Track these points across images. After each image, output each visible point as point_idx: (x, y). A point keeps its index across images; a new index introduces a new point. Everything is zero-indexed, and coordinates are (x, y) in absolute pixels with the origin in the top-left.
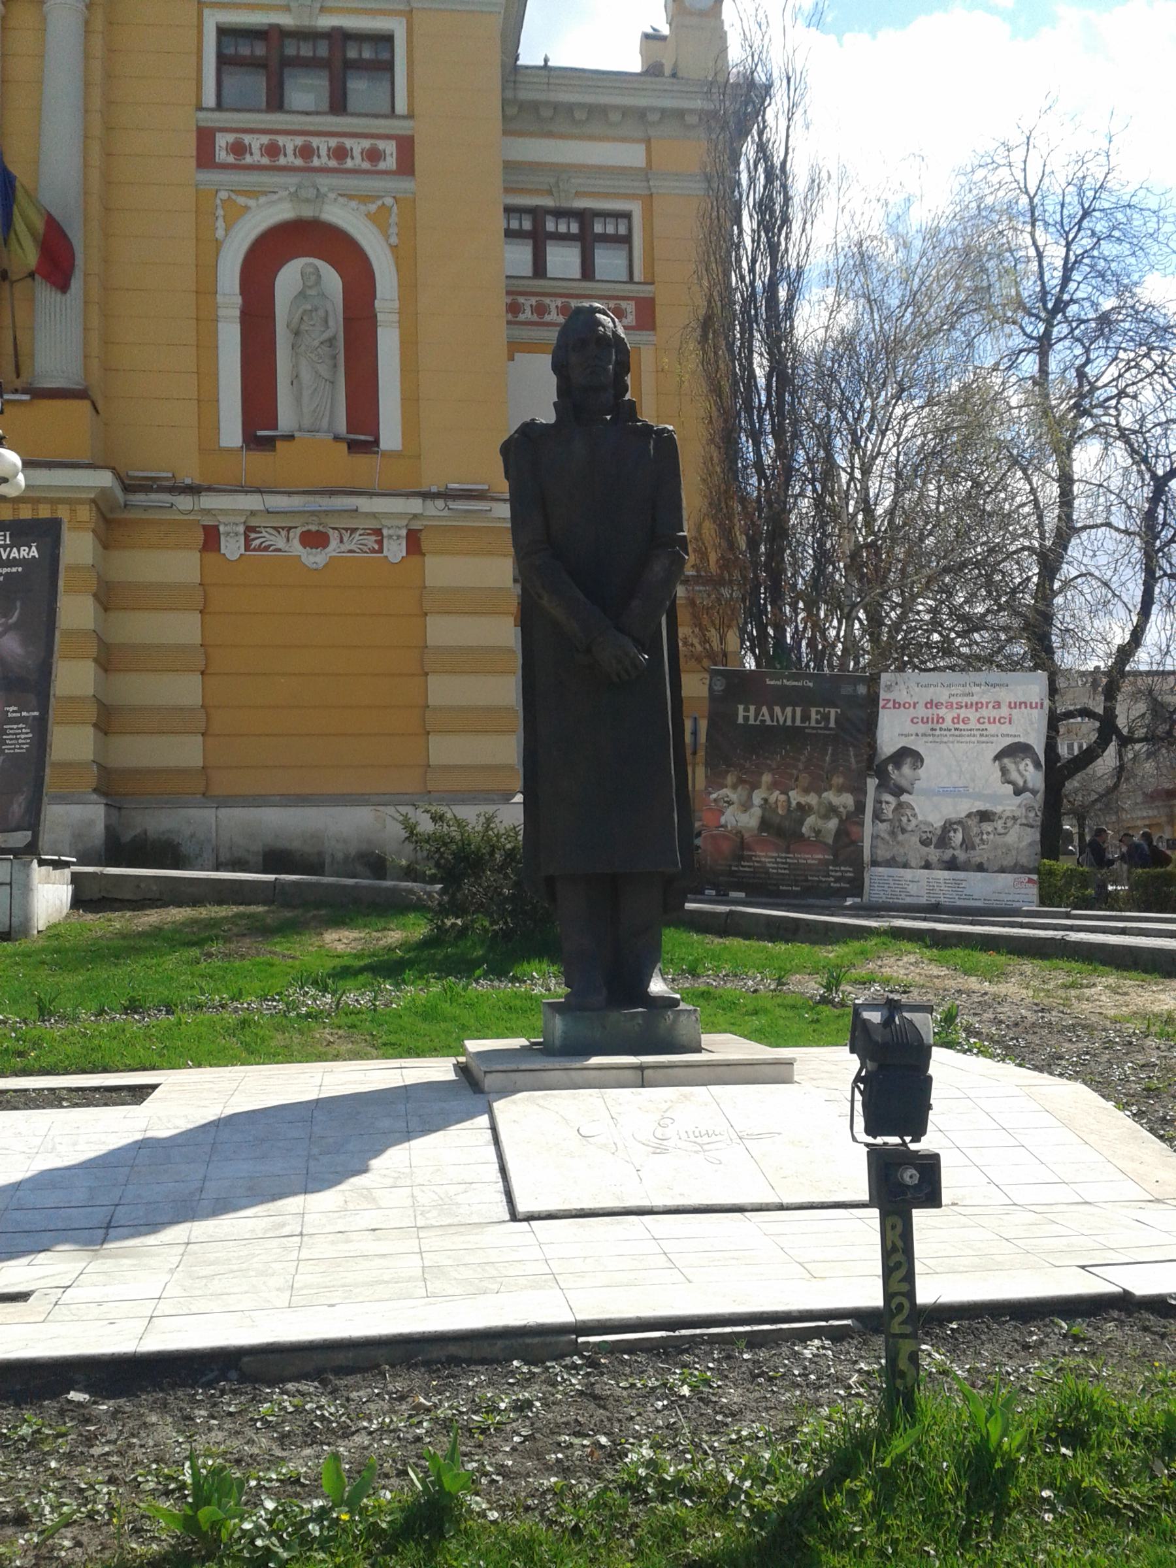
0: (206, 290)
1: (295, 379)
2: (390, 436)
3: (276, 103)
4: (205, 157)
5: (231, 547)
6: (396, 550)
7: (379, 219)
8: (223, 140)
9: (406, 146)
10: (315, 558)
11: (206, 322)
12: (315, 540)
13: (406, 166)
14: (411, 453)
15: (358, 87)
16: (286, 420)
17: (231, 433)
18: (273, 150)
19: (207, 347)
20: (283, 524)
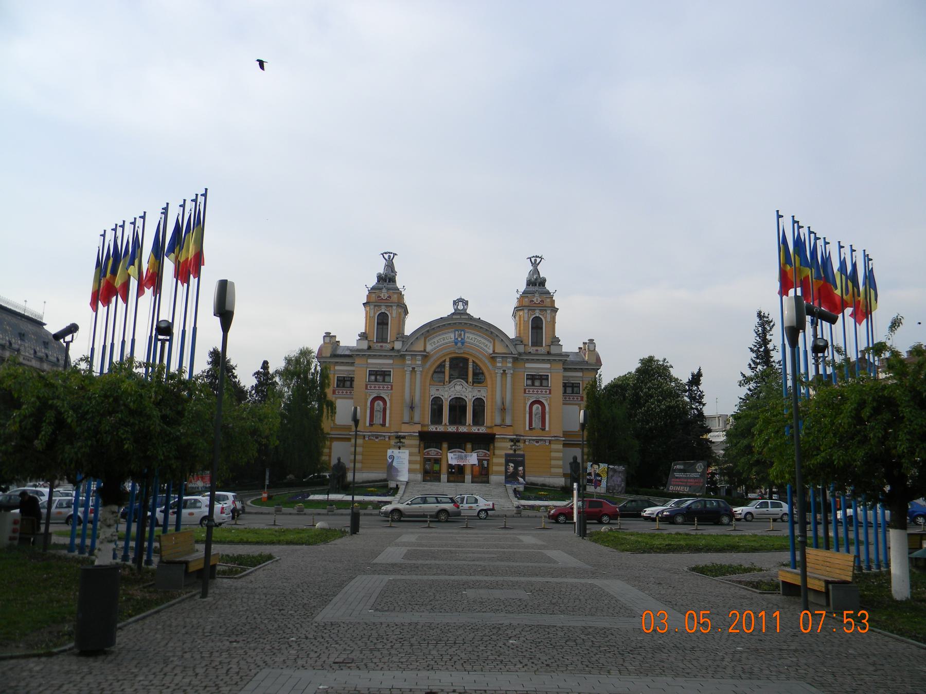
0: (525, 410)
1: (535, 421)
2: (547, 429)
3: (533, 385)
4: (525, 392)
5: (527, 443)
6: (547, 444)
7: (546, 400)
8: (527, 390)
9: (550, 390)
10: (537, 444)
11: (525, 414)
12: (537, 442)
13: (550, 393)
14: (550, 431)
15: (544, 382)
16: (534, 426)
17: (527, 428)
18: (533, 391)
19: (525, 417)
20: (534, 440)
